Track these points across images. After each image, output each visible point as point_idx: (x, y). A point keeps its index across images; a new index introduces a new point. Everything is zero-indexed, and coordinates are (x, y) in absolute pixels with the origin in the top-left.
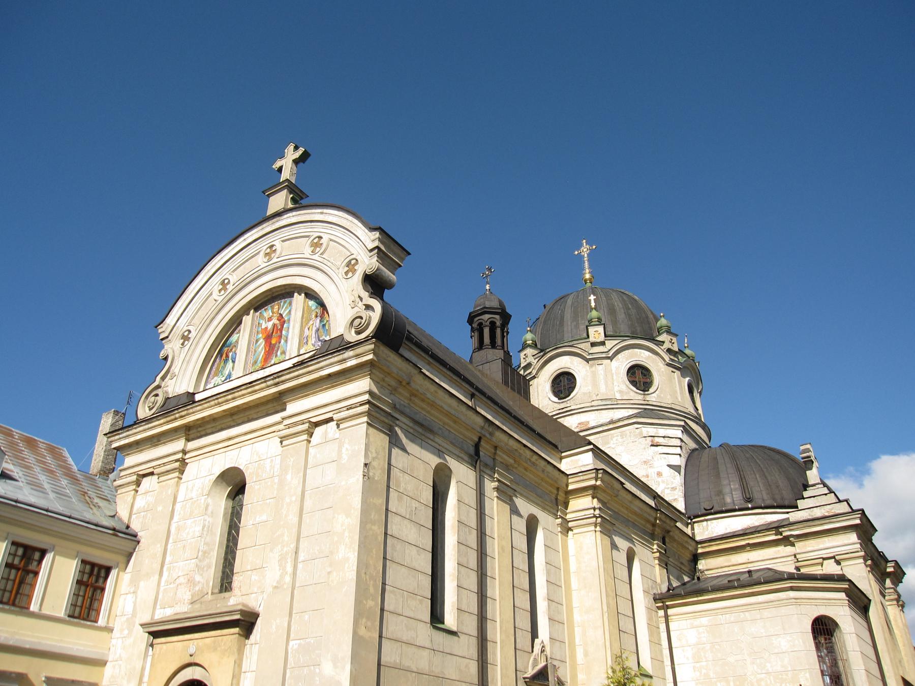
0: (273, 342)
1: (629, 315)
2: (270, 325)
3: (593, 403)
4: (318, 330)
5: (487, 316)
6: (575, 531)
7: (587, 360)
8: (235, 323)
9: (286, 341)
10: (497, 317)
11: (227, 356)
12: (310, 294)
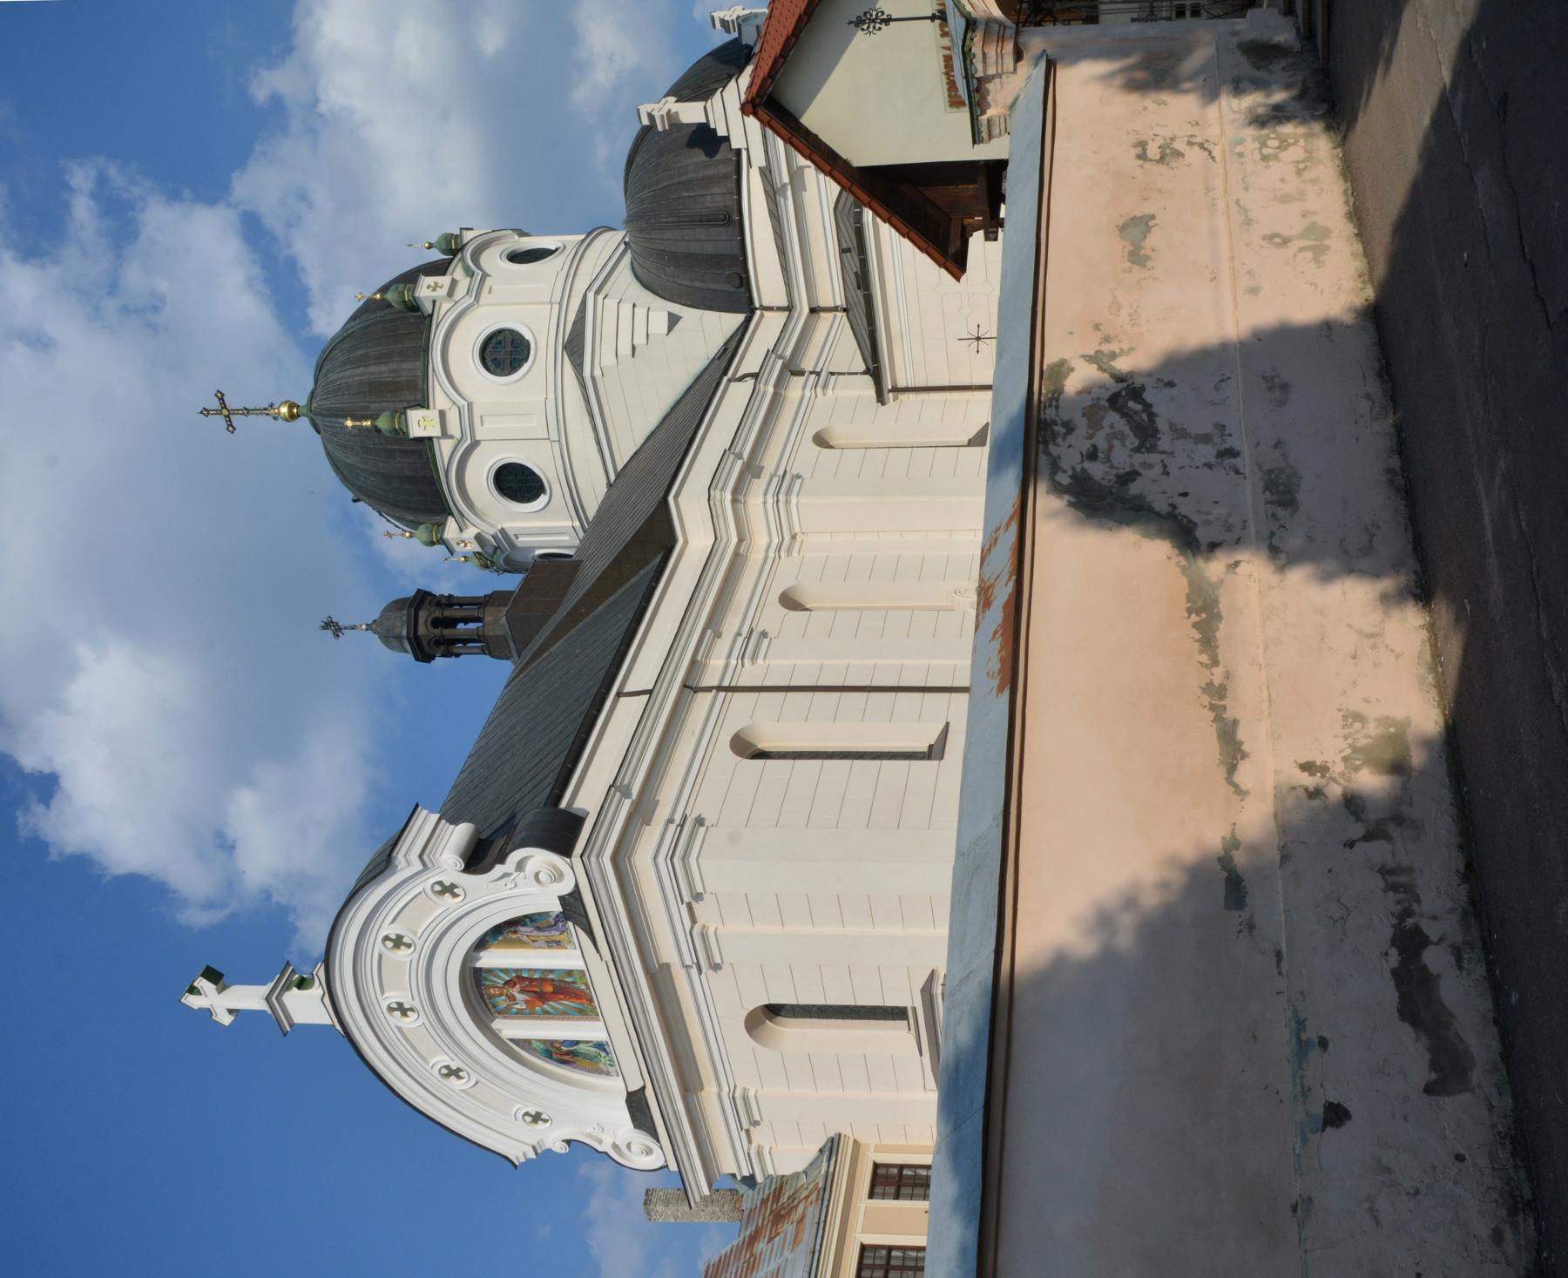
0: (549, 989)
1: (381, 359)
2: (520, 997)
3: (554, 436)
4: (539, 929)
5: (422, 630)
6: (797, 529)
7: (475, 444)
8: (515, 1049)
9: (551, 971)
10: (422, 615)
11: (568, 1053)
12: (481, 944)
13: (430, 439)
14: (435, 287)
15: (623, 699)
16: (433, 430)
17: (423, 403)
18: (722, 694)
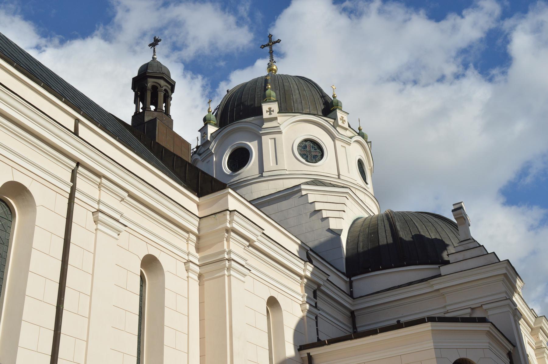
13: (262, 114)
14: (342, 119)
15: (73, 121)
16: (266, 115)
17: (281, 111)
18: (69, 190)
